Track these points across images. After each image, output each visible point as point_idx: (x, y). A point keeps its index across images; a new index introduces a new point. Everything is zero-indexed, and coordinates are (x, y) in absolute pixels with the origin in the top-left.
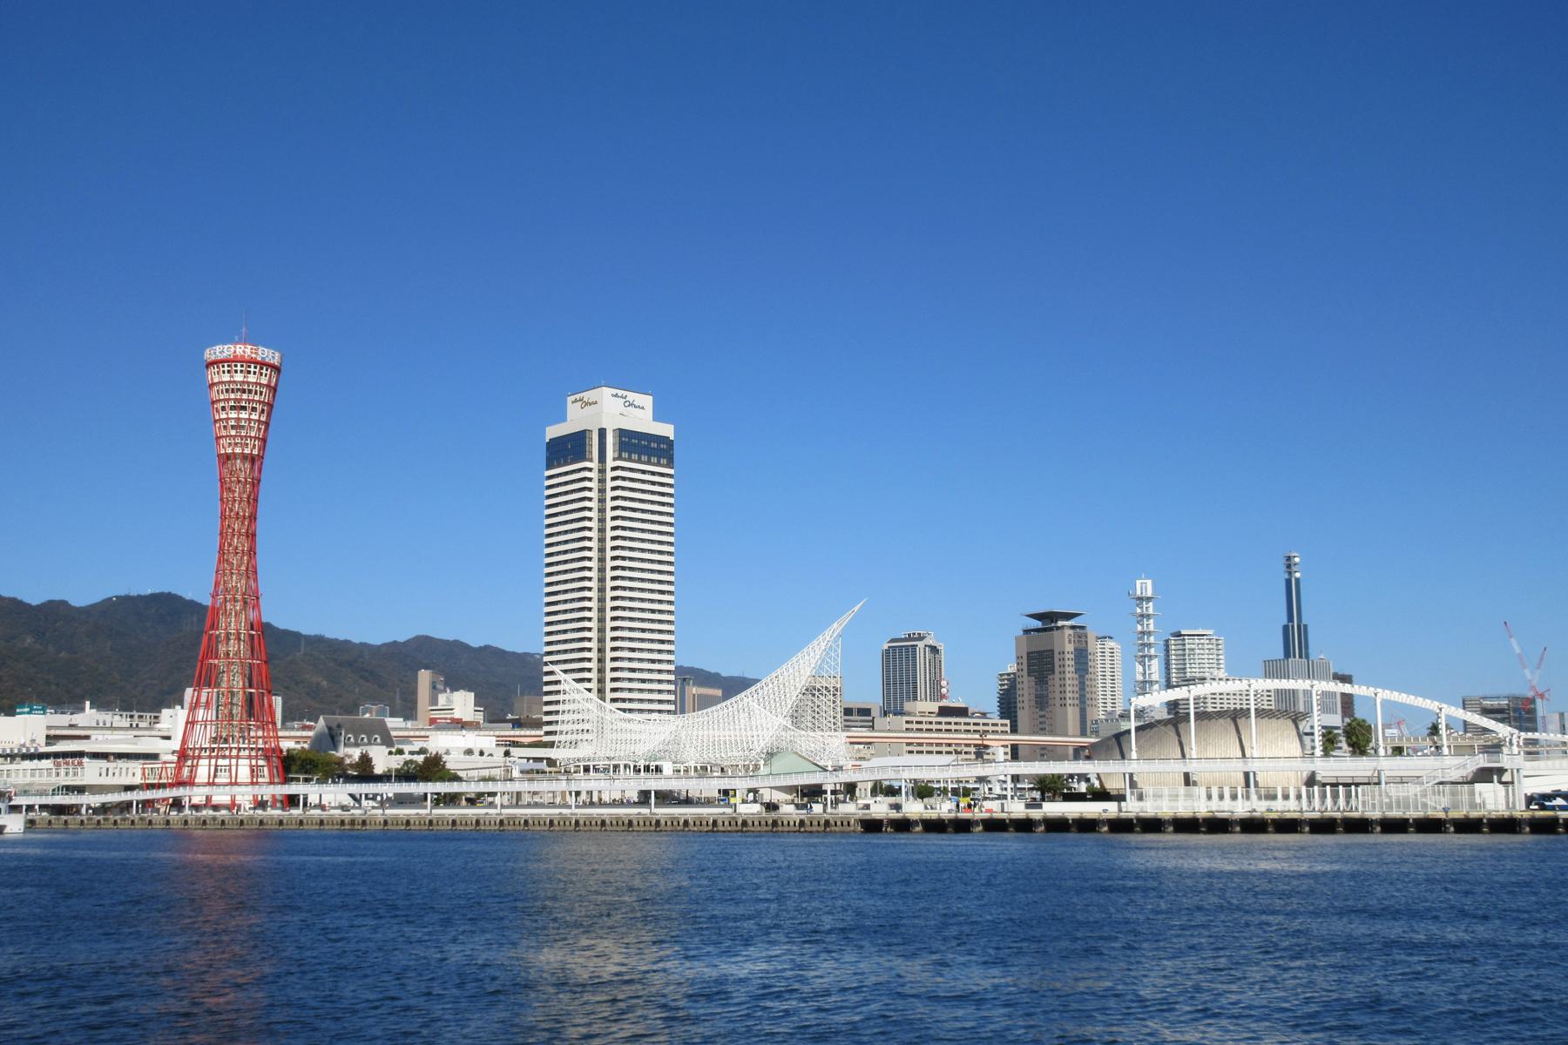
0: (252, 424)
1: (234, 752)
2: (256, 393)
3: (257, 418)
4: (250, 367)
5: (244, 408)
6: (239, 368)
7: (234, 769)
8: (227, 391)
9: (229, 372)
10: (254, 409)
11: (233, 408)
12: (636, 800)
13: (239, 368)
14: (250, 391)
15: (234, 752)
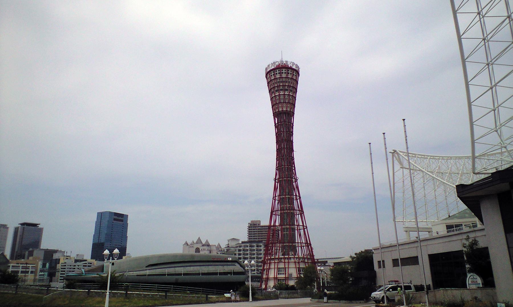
0: (291, 98)
1: (286, 261)
2: (291, 83)
3: (292, 94)
4: (283, 70)
5: (287, 90)
6: (278, 72)
7: (287, 269)
8: (279, 82)
9: (279, 73)
10: (291, 91)
11: (281, 90)
12: (430, 282)
13: (284, 71)
14: (289, 82)
15: (286, 261)
